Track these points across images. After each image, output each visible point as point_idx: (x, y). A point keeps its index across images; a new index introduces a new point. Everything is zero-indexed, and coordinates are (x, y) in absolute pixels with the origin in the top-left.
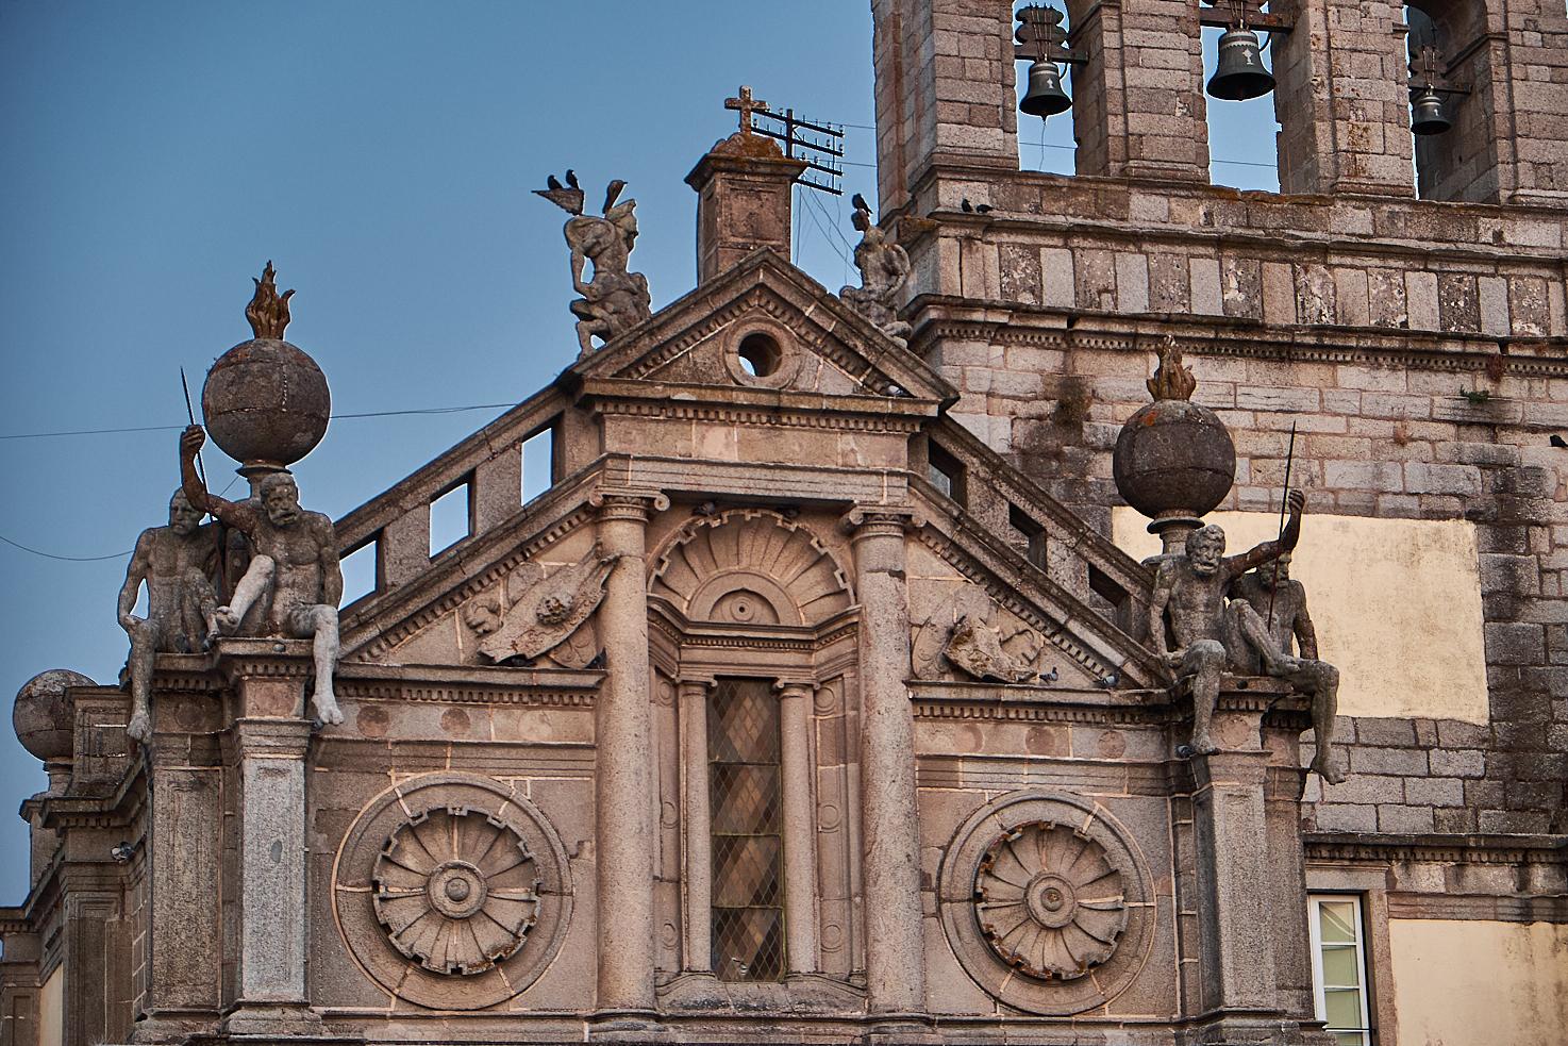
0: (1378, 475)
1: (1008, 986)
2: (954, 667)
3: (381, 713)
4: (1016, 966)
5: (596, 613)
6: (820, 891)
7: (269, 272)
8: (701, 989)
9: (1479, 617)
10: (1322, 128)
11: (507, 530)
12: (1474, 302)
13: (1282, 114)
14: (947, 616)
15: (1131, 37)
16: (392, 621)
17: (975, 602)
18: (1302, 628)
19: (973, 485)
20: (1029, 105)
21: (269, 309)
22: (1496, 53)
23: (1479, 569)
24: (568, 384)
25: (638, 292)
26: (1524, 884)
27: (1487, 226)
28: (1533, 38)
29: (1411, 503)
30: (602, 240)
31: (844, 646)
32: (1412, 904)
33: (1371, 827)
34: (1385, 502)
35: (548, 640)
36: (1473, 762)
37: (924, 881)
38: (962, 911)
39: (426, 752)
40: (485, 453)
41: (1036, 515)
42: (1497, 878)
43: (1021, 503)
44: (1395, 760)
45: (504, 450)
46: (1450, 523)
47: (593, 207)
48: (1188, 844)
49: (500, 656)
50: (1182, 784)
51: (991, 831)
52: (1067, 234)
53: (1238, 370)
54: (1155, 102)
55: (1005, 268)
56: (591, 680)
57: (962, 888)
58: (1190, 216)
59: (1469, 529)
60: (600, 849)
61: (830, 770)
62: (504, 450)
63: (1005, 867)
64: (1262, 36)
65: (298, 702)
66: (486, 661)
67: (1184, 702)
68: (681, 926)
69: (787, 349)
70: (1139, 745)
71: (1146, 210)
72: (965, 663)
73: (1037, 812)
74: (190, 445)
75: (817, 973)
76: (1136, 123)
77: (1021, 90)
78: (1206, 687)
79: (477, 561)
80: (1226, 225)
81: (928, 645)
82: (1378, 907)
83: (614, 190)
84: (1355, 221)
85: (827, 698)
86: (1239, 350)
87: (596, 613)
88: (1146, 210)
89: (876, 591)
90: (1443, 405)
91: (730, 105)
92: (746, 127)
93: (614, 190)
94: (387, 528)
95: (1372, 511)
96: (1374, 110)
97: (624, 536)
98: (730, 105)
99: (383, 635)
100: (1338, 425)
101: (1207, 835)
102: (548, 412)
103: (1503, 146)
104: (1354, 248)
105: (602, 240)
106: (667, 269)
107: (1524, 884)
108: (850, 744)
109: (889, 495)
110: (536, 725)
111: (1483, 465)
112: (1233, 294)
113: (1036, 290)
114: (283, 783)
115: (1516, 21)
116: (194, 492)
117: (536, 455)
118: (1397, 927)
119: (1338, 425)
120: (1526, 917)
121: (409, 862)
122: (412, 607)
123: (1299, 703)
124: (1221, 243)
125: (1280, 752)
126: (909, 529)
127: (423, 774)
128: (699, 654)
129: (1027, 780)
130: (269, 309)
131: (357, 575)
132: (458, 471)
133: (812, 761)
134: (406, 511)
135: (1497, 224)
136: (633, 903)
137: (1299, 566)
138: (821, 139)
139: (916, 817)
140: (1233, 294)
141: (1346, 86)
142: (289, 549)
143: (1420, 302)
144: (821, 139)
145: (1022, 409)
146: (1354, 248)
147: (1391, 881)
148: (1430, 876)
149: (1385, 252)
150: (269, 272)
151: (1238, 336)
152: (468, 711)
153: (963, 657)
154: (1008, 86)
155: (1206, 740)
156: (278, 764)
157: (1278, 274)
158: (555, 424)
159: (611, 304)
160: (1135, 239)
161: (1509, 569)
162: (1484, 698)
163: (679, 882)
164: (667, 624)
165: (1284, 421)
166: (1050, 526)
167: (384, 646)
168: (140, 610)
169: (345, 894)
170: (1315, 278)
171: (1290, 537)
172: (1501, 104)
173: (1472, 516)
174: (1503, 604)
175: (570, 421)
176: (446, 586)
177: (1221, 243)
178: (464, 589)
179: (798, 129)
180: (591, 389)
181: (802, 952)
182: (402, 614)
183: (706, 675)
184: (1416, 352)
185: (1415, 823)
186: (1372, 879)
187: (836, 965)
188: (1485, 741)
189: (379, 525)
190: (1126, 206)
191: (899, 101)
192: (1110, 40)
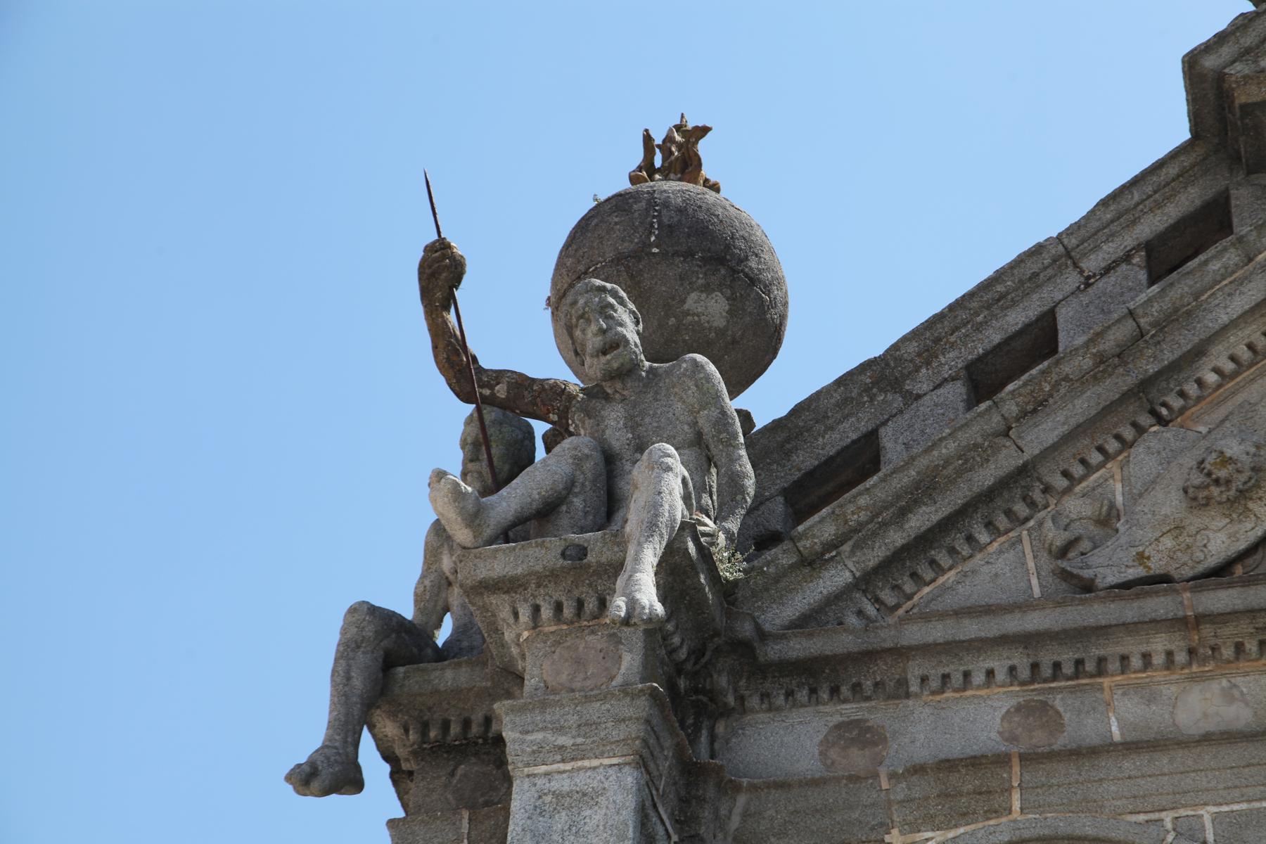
3: (869, 729)
11: (1101, 359)
16: (875, 555)
35: (1220, 539)
40: (1072, 280)
45: (1108, 270)
62: (1108, 270)
79: (1048, 425)
94: (882, 431)
99: (865, 582)
114: (594, 817)
122: (920, 520)
127: (962, 830)
134: (919, 397)
142: (632, 424)
152: (1058, 702)
156: (582, 780)
167: (870, 610)
176: (986, 476)
182: (897, 538)
189: (865, 426)
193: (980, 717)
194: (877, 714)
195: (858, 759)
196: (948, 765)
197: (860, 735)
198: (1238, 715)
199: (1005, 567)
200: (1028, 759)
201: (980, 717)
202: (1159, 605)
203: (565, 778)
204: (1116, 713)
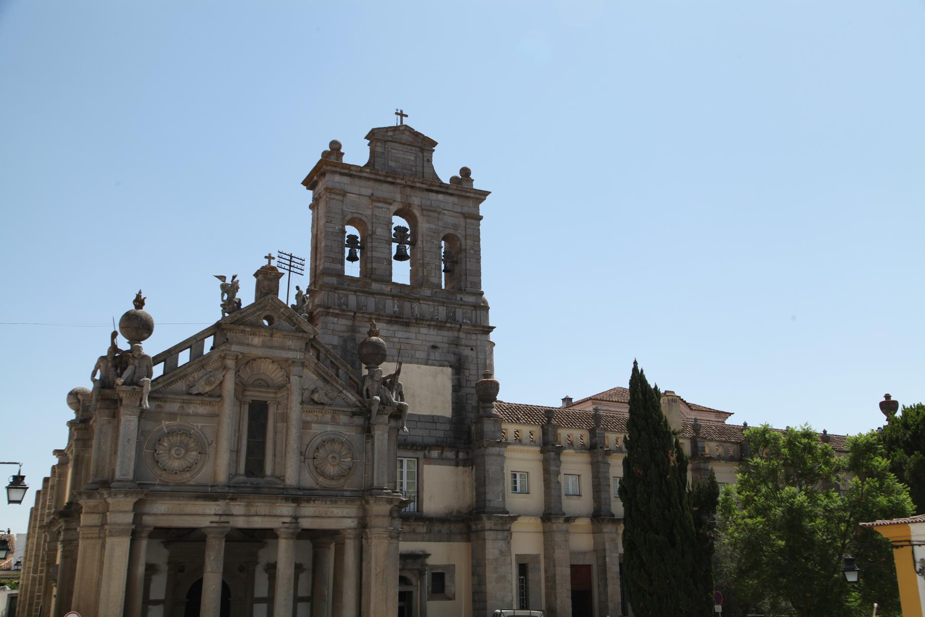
0: (429, 355)
1: (321, 479)
2: (313, 400)
4: (323, 474)
5: (221, 383)
6: (275, 455)
7: (140, 292)
8: (242, 478)
9: (451, 391)
10: (420, 269)
12: (454, 314)
13: (411, 265)
14: (312, 387)
15: (375, 244)
17: (320, 383)
18: (401, 395)
19: (322, 355)
20: (348, 259)
21: (139, 302)
22: (463, 255)
23: (452, 380)
24: (218, 326)
25: (239, 303)
26: (457, 456)
27: (459, 297)
28: (472, 252)
29: (437, 363)
30: (230, 289)
31: (285, 393)
32: (429, 460)
33: (421, 441)
34: (430, 362)
35: (208, 389)
36: (447, 427)
37: (301, 454)
38: (310, 461)
39: (172, 416)
41: (337, 363)
42: (450, 454)
43: (333, 360)
44: (428, 425)
46: (445, 368)
47: (229, 281)
48: (369, 445)
49: (195, 392)
50: (367, 431)
51: (319, 440)
52: (355, 292)
53: (395, 327)
54: (380, 260)
55: (340, 299)
56: (218, 399)
57: (311, 456)
58: (387, 289)
59: (450, 370)
60: (217, 443)
61: (280, 425)
63: (321, 451)
64: (407, 246)
65: (138, 403)
66: (191, 394)
67: (370, 411)
68: (237, 463)
69: (276, 319)
70: (359, 420)
71: (375, 286)
72: (316, 399)
73: (332, 436)
74: (114, 335)
75: (273, 476)
76: (375, 265)
77: (347, 255)
78: (375, 409)
80: (395, 292)
81: (307, 394)
82: (421, 461)
83: (234, 277)
84: (427, 292)
85: (280, 406)
86: (396, 323)
87: (221, 383)
88: (375, 286)
89: (294, 380)
90: (445, 339)
91: (266, 257)
92: (269, 263)
93: (234, 277)
95: (427, 364)
96: (433, 266)
97: (230, 363)
98: (266, 257)
100: (420, 342)
101: (373, 445)
102: (212, 331)
103: (464, 277)
104: (427, 299)
105: (230, 289)
106: (247, 296)
107: (457, 456)
108: (285, 418)
109: (299, 356)
110: (202, 410)
111: (454, 354)
112: (396, 309)
113: (347, 305)
114: (132, 423)
115: (468, 247)
116: (114, 348)
117: (209, 342)
118: (426, 467)
119: (420, 342)
120: (457, 465)
121: (166, 444)
122: (172, 379)
123: (399, 413)
124: (394, 296)
125: (393, 423)
126: (303, 365)
128: (248, 393)
129: (329, 428)
130: (139, 302)
131: (158, 370)
132: (187, 345)
133: (275, 422)
135: (461, 296)
136: (224, 458)
137: (401, 380)
138: (299, 261)
139: (301, 438)
140: (396, 309)
141: (427, 260)
143: (442, 312)
144: (299, 261)
145: (341, 334)
146: (427, 299)
147: (425, 457)
148: (435, 454)
149: (434, 301)
150: (140, 292)
151: (396, 319)
153: (316, 397)
154: (343, 254)
155: (373, 420)
157: (407, 305)
158: (214, 334)
159: (231, 305)
160: (372, 294)
161: (459, 380)
162: (450, 411)
163: (238, 452)
164: (241, 387)
165: (406, 341)
166: (340, 366)
168: (97, 377)
169: (147, 451)
170: (416, 306)
171: (398, 372)
172: (464, 268)
173: (451, 366)
174: (457, 388)
175: (218, 333)
176: (182, 374)
177: (394, 296)
178: (185, 376)
179: (294, 259)
180: (224, 327)
181: (268, 470)
183: (249, 399)
184: (440, 326)
185: (432, 441)
186: (420, 454)
187: (277, 473)
188: (450, 421)
190: (370, 285)
191: (316, 255)
192: (369, 245)
193: (175, 407)
194: (162, 404)
195: (159, 410)
196: (171, 413)
197: (159, 406)
198: (205, 412)
199: (181, 386)
200: (182, 415)
201: (175, 407)
202: (200, 398)
203: (129, 418)
204: (191, 409)
